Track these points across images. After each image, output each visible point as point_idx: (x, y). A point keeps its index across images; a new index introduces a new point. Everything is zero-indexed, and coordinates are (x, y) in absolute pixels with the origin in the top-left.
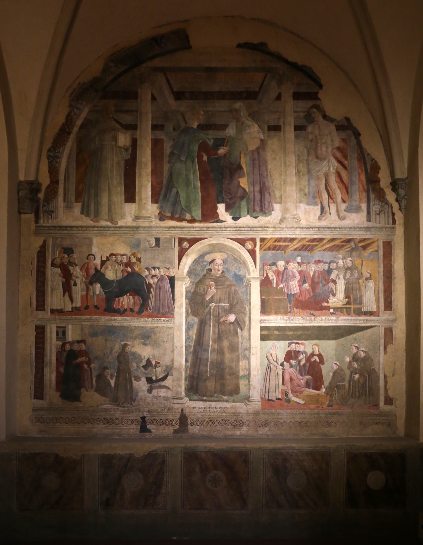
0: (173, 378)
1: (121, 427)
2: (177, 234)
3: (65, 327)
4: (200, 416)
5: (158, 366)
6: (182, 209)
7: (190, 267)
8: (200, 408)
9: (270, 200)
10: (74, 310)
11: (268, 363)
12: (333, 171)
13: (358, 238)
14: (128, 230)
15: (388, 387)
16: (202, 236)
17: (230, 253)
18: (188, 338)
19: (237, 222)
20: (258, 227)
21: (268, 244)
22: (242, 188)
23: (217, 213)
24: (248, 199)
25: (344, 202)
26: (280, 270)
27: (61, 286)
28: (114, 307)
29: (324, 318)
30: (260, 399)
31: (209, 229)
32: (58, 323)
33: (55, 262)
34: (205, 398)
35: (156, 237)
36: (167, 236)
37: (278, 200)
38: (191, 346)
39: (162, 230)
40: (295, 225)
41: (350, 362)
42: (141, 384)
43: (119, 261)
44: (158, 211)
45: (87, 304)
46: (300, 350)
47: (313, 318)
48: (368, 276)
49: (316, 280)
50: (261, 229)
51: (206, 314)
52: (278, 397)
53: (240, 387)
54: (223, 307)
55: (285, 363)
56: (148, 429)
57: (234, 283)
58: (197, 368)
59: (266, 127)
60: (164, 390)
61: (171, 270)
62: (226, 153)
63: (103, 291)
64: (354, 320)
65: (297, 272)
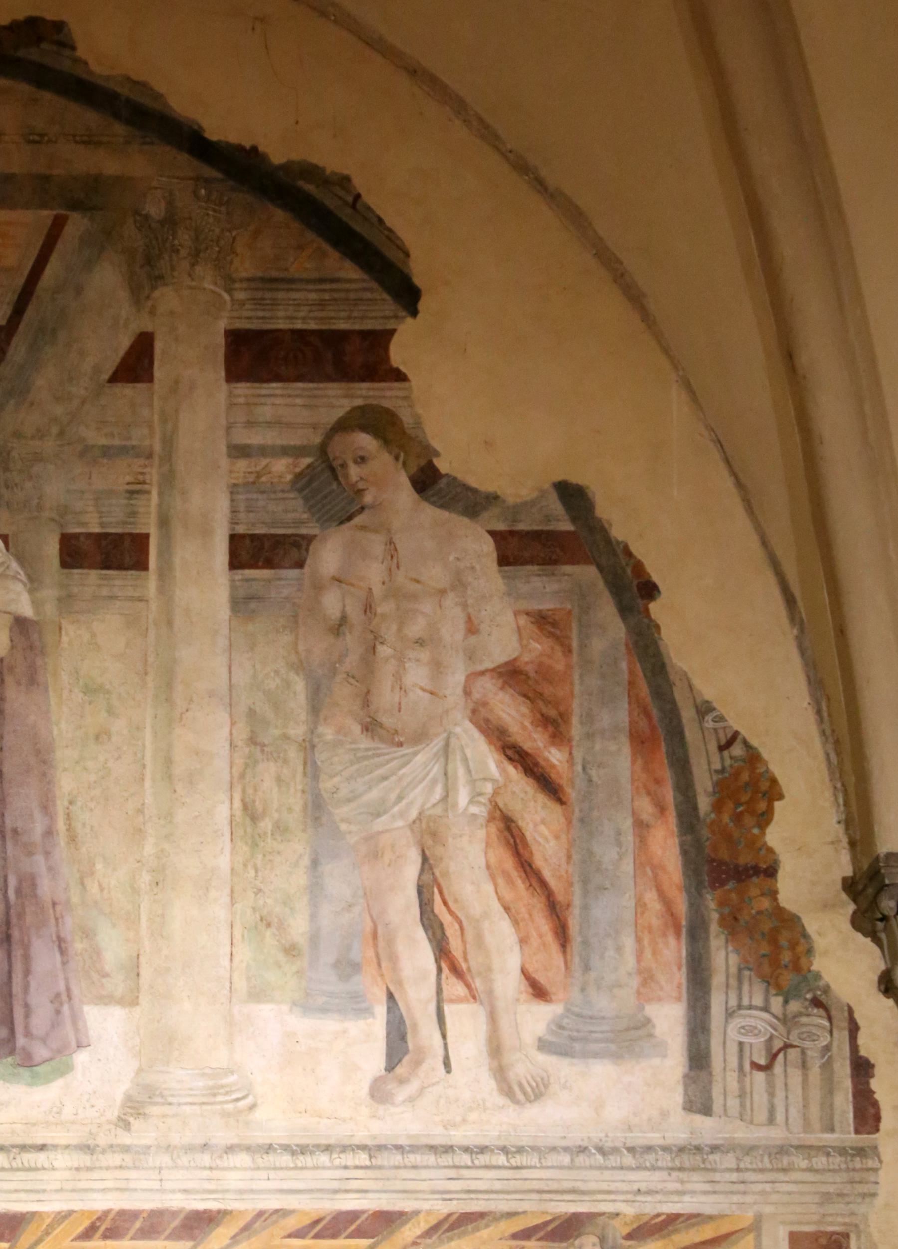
9: (62, 987)
12: (474, 809)
13: (628, 1210)
25: (539, 992)
37: (117, 984)
40: (222, 1136)
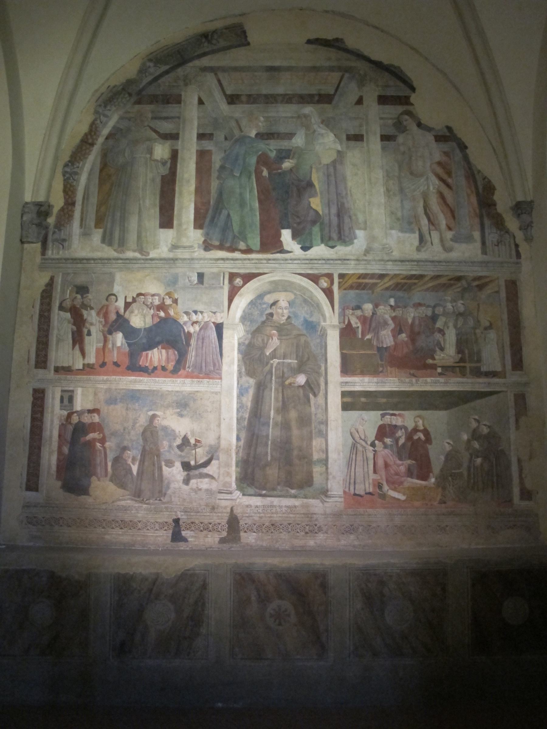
0: (219, 463)
1: (144, 533)
2: (227, 268)
3: (72, 391)
4: (256, 518)
5: (198, 446)
6: (234, 237)
7: (244, 311)
8: (257, 507)
9: (351, 226)
10: (86, 368)
11: (353, 442)
12: (434, 191)
13: (471, 275)
14: (162, 263)
15: (523, 476)
16: (261, 271)
17: (298, 293)
18: (240, 406)
19: (307, 253)
20: (336, 260)
21: (350, 282)
22: (314, 209)
23: (281, 242)
24: (322, 224)
25: (450, 229)
26: (366, 315)
27: (70, 336)
28: (141, 363)
29: (429, 380)
30: (342, 493)
31: (270, 262)
32: (63, 385)
33: (64, 305)
34: (264, 492)
35: (199, 271)
36: (214, 271)
38: (245, 419)
39: (208, 263)
40: (386, 258)
41: (469, 441)
42: (175, 472)
43: (149, 303)
44: (203, 239)
45: (104, 360)
46: (397, 424)
47: (414, 380)
48: (488, 324)
49: (416, 329)
50: (339, 262)
51: (265, 374)
52: (368, 491)
53: (314, 475)
54: (289, 364)
55: (376, 442)
56: (182, 537)
57: (305, 332)
58: (253, 448)
59: (344, 137)
60: (206, 480)
61: (218, 314)
62: (293, 167)
63: (127, 342)
64: (472, 383)
65: (390, 319)
